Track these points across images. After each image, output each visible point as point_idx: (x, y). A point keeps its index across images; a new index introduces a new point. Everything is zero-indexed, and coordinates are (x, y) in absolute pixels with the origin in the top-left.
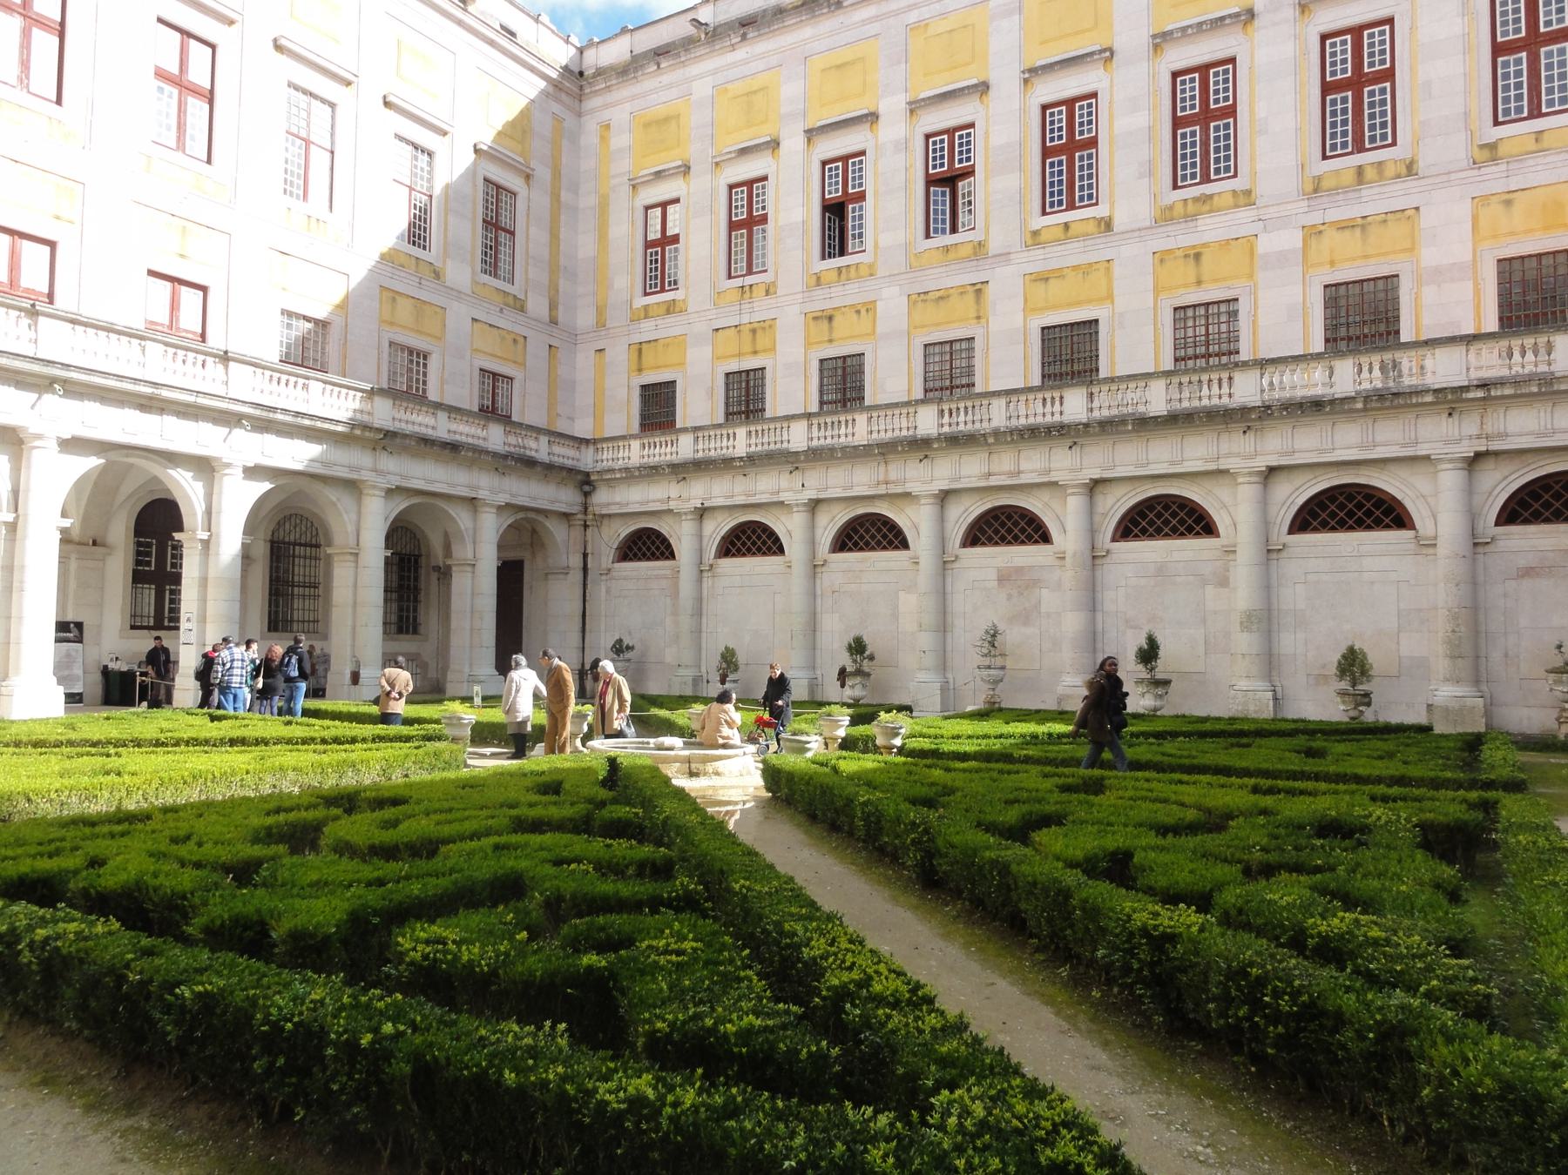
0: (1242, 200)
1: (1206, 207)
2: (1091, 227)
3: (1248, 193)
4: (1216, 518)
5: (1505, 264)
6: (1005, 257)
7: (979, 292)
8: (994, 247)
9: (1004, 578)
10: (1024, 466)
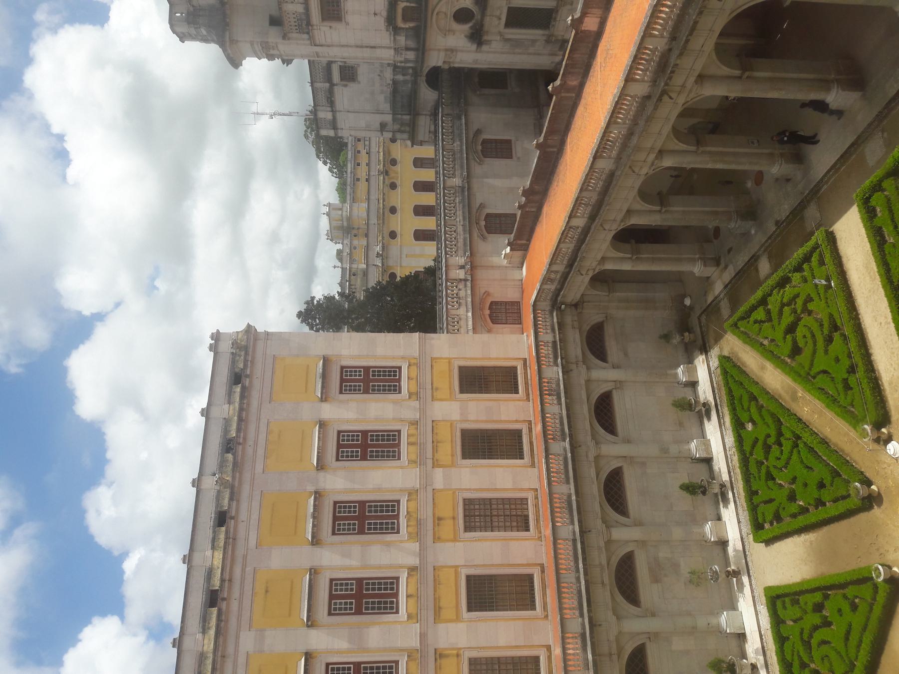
0: (414, 496)
1: (415, 515)
2: (413, 580)
3: (410, 494)
4: (614, 467)
5: (462, 392)
6: (423, 636)
7: (441, 656)
8: (415, 643)
9: (656, 579)
10: (597, 562)
